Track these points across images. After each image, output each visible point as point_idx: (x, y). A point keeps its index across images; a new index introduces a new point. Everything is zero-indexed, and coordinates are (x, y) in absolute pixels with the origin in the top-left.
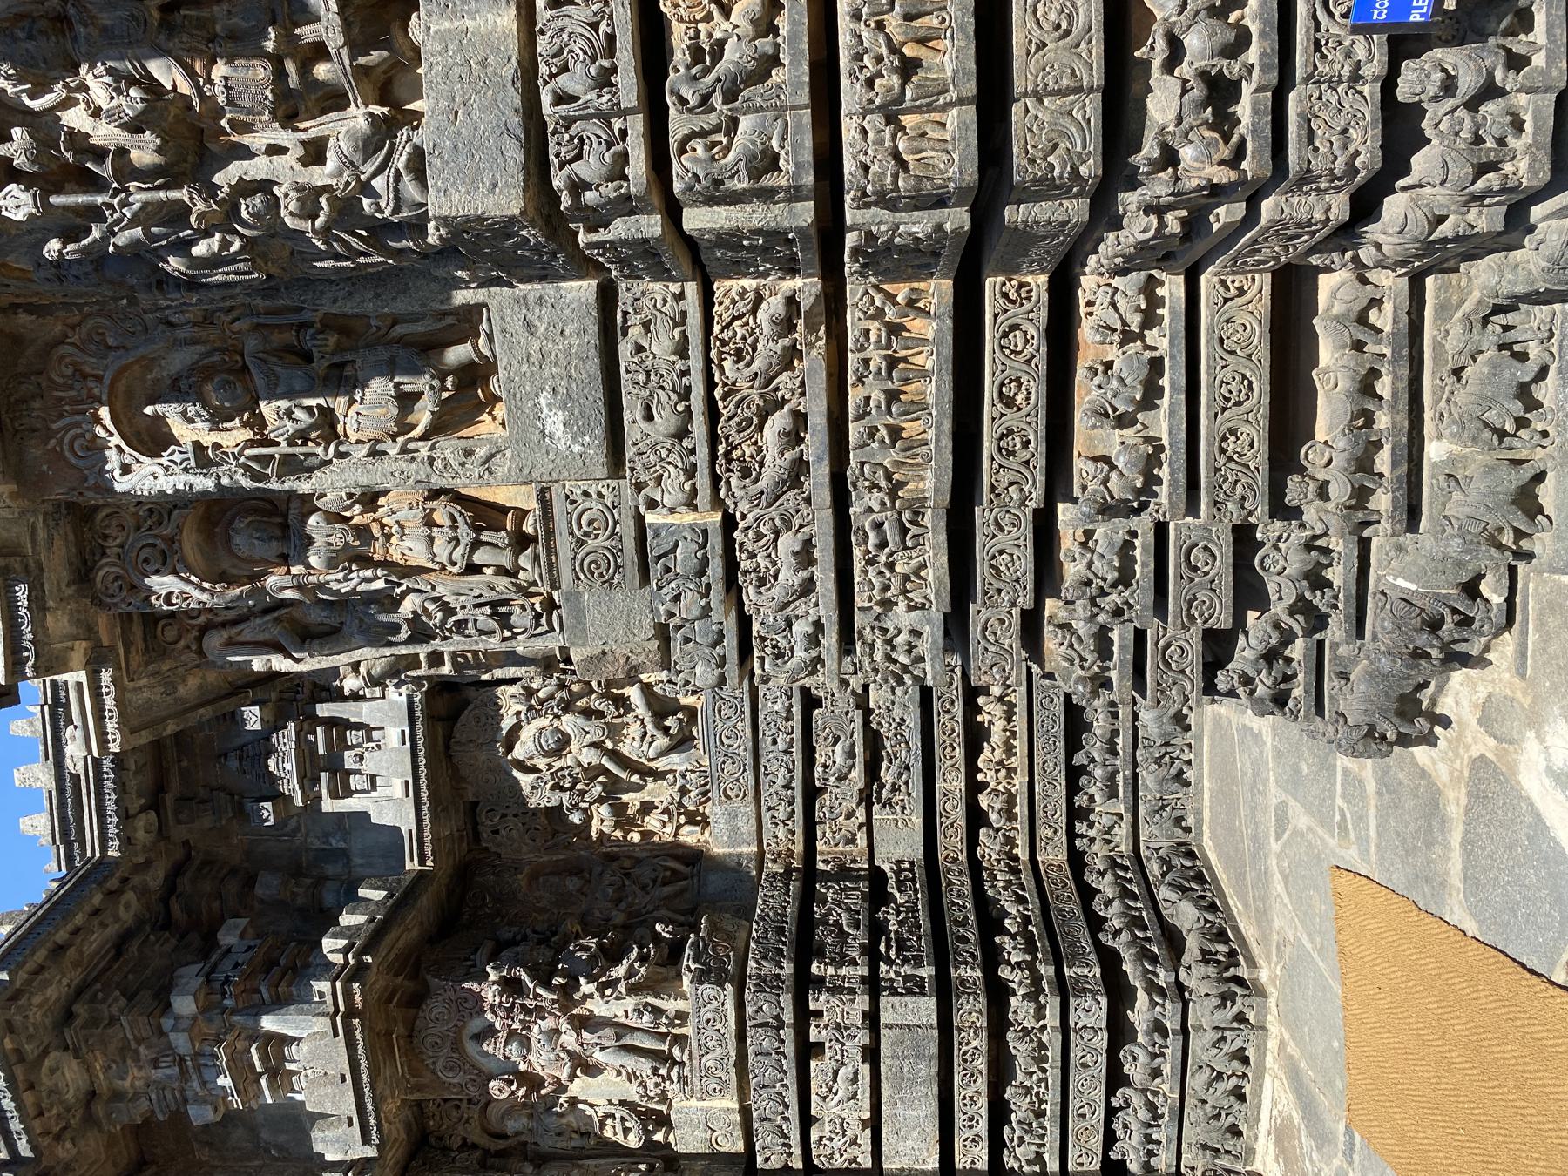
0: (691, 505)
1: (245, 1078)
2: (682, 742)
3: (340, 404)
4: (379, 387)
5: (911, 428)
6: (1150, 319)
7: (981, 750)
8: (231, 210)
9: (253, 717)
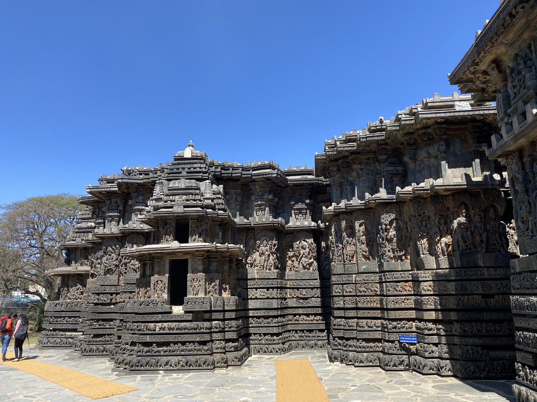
1: (260, 205)
2: (304, 268)
3: (365, 245)
4: (367, 249)
5: (365, 303)
6: (377, 327)
8: (384, 245)
9: (308, 201)
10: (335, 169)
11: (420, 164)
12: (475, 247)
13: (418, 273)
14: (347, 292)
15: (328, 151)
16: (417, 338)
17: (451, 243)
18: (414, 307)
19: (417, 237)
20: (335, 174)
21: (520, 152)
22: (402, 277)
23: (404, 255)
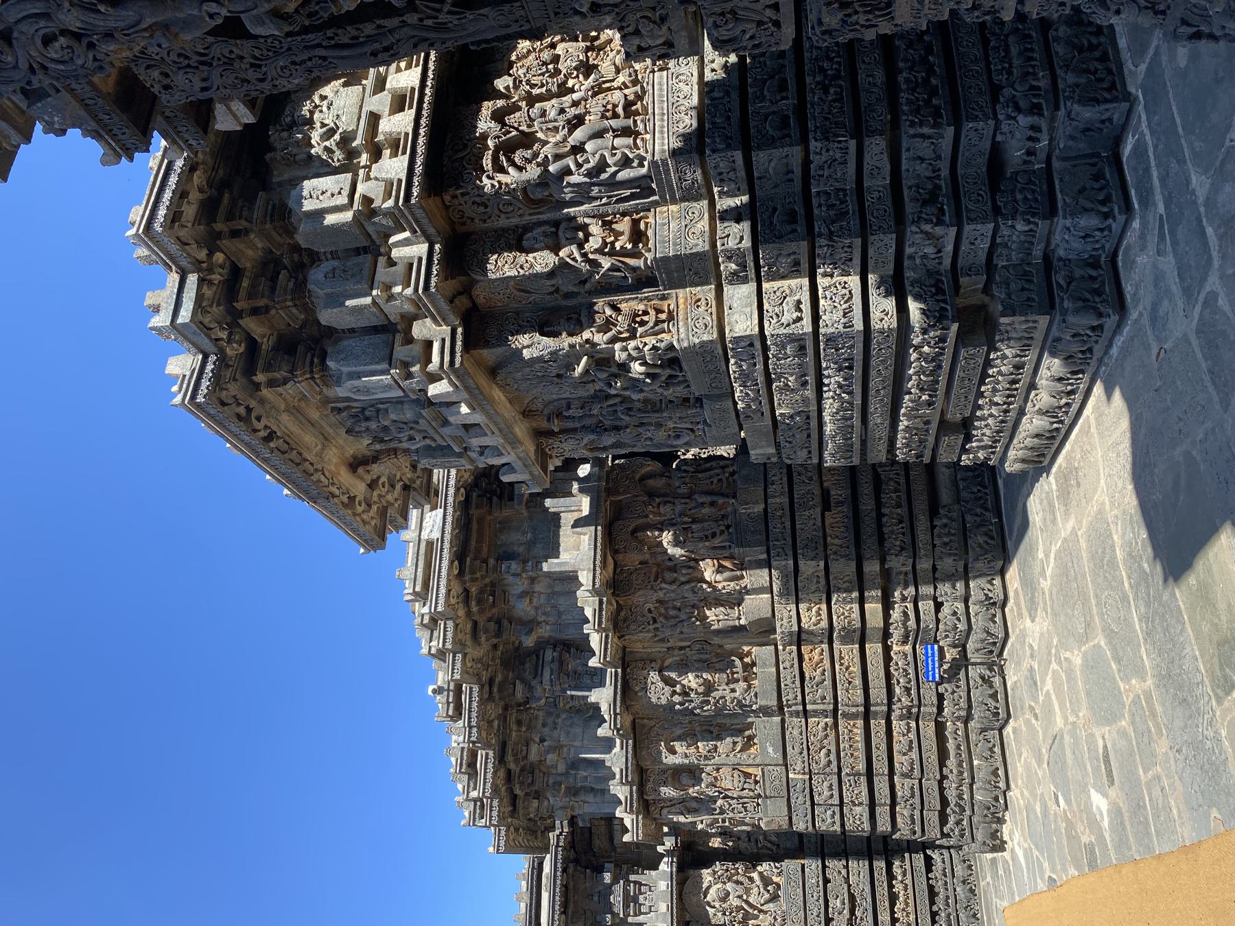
2: (774, 898)
4: (729, 740)
5: (856, 754)
6: (909, 731)
8: (718, 701)
9: (607, 877)
10: (535, 803)
11: (544, 614)
12: (724, 517)
13: (782, 633)
15: (490, 820)
16: (927, 644)
17: (715, 561)
18: (857, 646)
19: (701, 629)
20: (546, 803)
21: (538, 434)
22: (792, 666)
23: (741, 659)
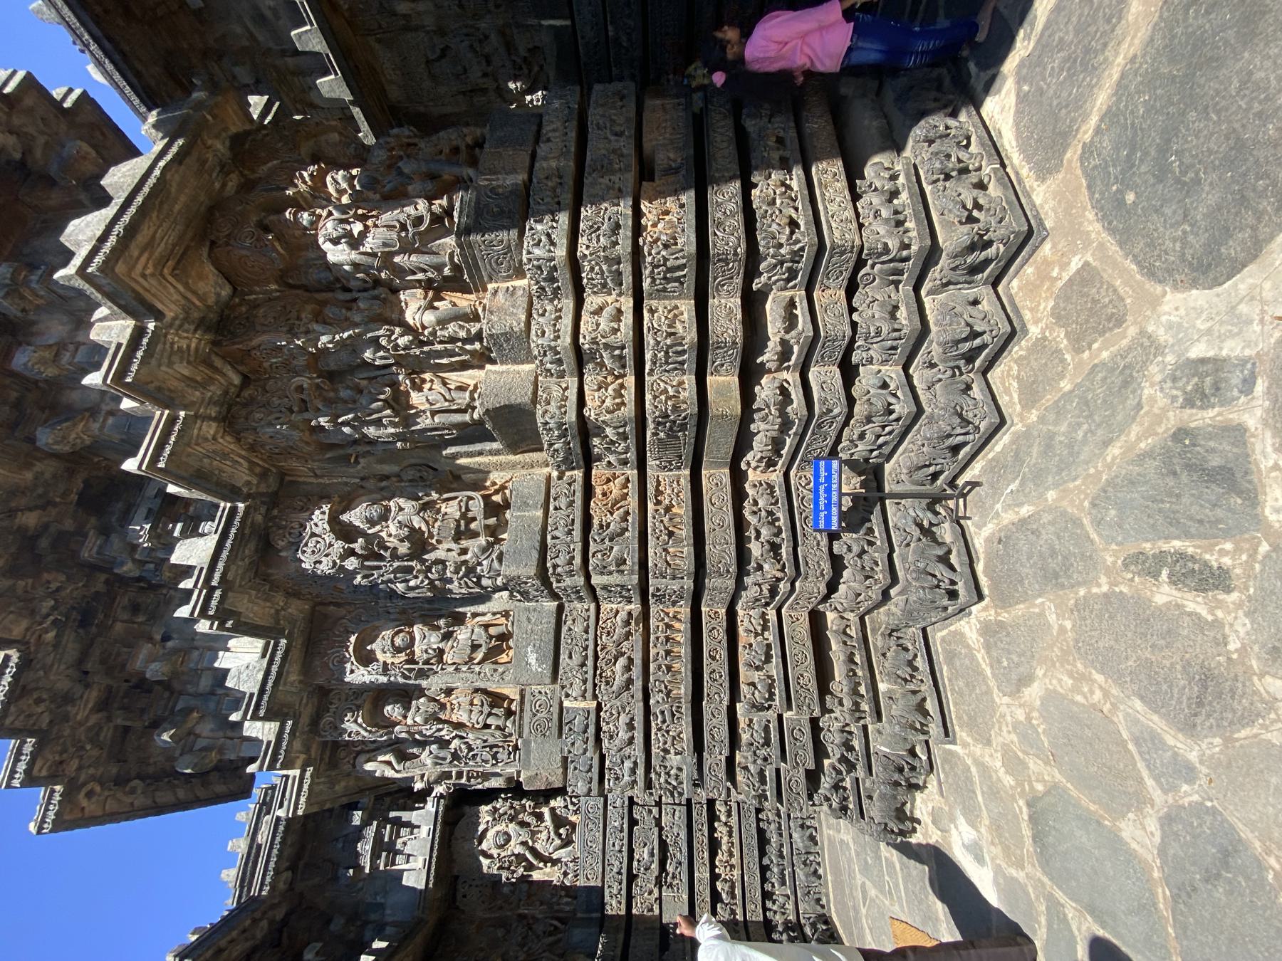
0: (584, 698)
2: (567, 843)
5: (676, 666)
6: (765, 628)
7: (717, 854)
9: (357, 817)
14: (632, 738)
18: (687, 472)
22: (571, 504)
